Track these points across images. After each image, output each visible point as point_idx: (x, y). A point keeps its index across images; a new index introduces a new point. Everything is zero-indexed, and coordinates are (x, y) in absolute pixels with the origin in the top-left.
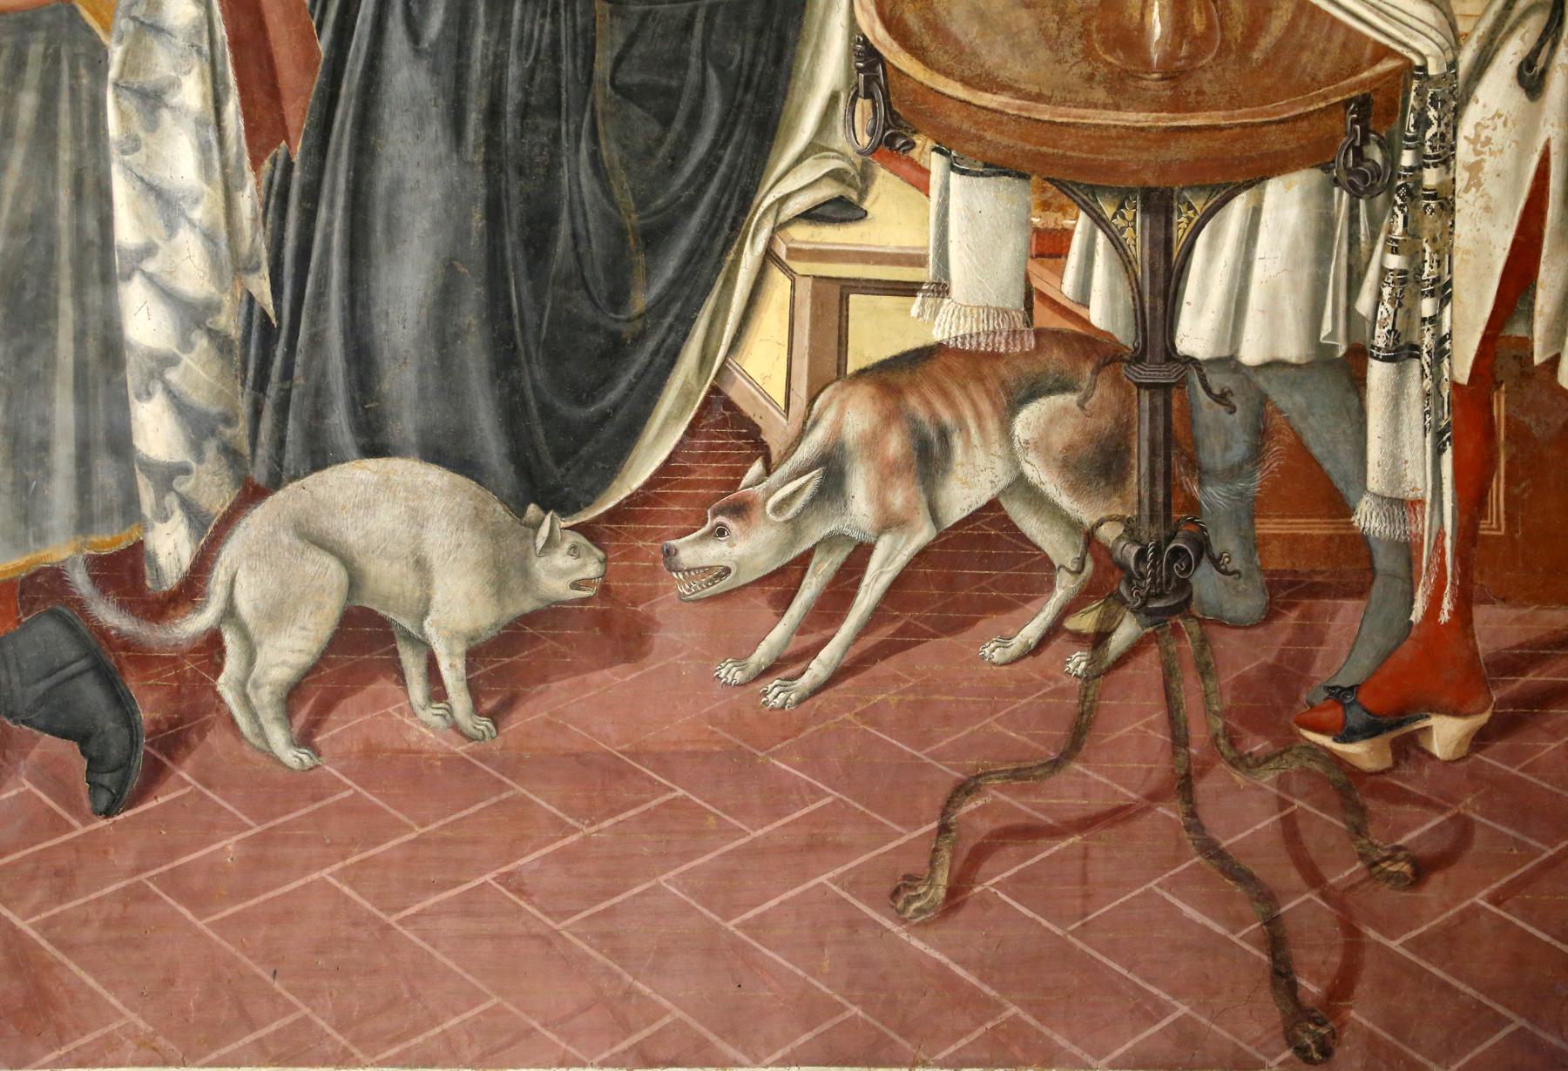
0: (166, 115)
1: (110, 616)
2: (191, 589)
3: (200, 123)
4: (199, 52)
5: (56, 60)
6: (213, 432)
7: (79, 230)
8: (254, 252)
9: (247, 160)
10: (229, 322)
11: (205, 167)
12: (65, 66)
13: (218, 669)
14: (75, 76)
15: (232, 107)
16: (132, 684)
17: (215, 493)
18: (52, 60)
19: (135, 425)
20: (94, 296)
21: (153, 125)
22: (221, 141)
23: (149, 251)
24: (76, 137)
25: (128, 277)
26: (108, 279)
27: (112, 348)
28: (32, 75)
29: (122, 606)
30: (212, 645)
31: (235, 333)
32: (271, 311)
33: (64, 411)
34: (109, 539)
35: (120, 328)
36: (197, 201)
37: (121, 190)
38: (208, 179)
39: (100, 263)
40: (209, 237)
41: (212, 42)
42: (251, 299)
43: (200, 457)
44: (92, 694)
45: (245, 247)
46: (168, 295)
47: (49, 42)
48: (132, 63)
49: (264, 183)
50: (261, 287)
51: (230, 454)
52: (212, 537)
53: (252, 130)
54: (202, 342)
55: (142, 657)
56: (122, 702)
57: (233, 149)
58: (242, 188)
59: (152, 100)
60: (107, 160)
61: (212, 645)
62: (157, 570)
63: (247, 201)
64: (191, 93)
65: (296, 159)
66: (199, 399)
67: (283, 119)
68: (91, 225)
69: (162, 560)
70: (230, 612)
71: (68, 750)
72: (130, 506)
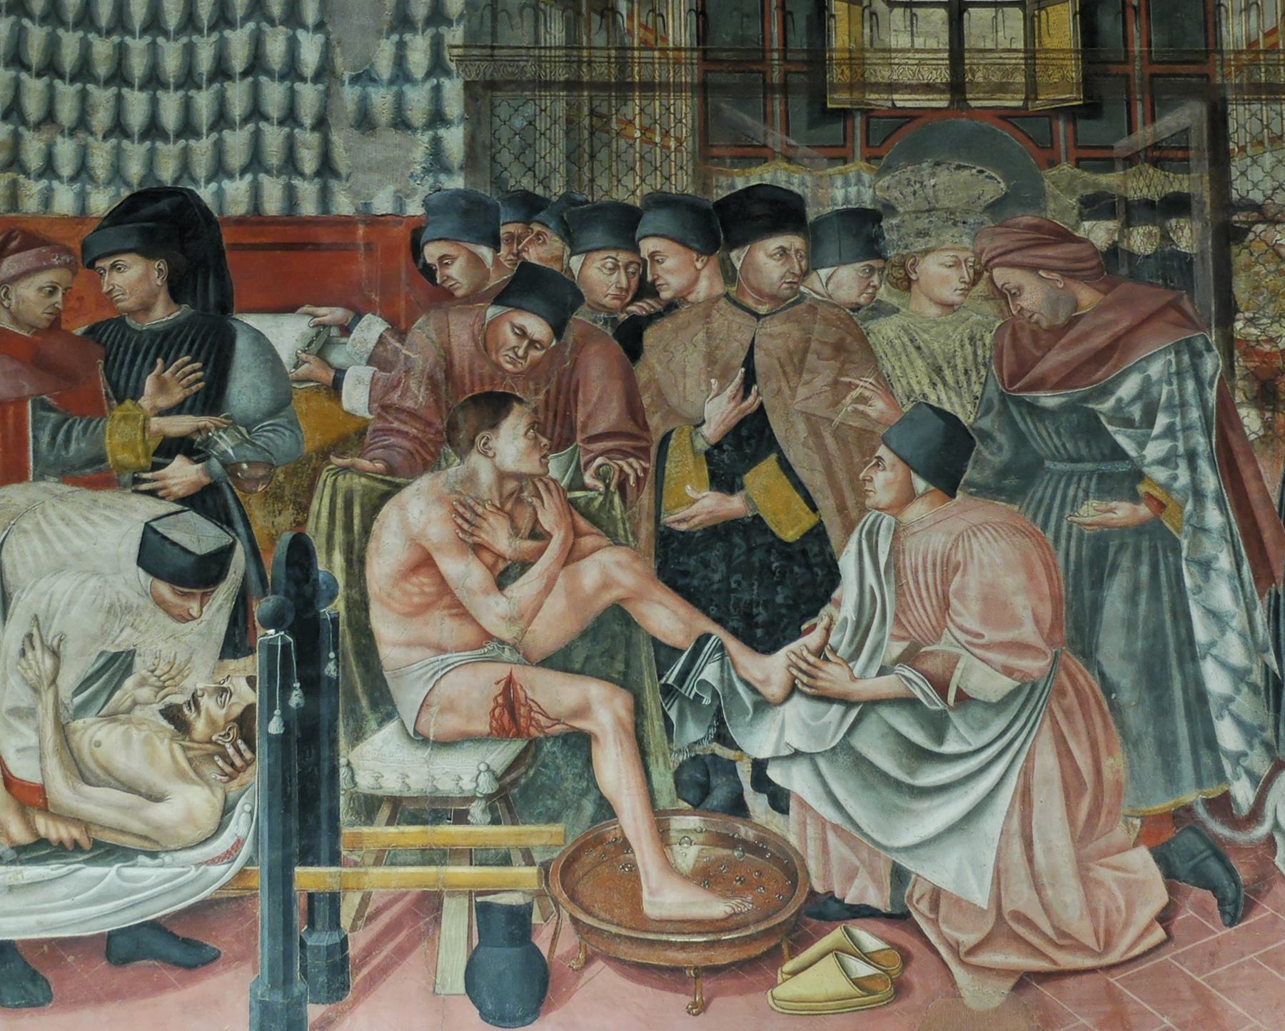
0: (1213, 574)
1: (1219, 829)
2: (1256, 814)
3: (1230, 577)
4: (1226, 541)
5: (1156, 549)
6: (1256, 735)
7: (1177, 634)
8: (1265, 643)
9: (1257, 598)
10: (1257, 677)
11: (1236, 599)
12: (1161, 553)
13: (1275, 853)
14: (1166, 557)
15: (1246, 568)
16: (1234, 862)
17: (1262, 765)
18: (1154, 550)
19: (1218, 733)
20: (1189, 667)
21: (1207, 577)
22: (1242, 586)
23: (1213, 644)
24: (1170, 588)
25: (1204, 658)
26: (1194, 659)
27: (1198, 695)
28: (1146, 558)
29: (1223, 823)
30: (1270, 842)
31: (1261, 684)
32: (1277, 672)
33: (1182, 729)
34: (1214, 791)
35: (1204, 684)
36: (1233, 617)
37: (1196, 613)
38: (1238, 605)
39: (1189, 651)
40: (1242, 635)
41: (1232, 535)
42: (1267, 666)
43: (1251, 747)
44: (1215, 868)
45: (1260, 639)
46: (1224, 665)
47: (1151, 540)
48: (1195, 546)
49: (1266, 603)
50: (1271, 658)
51: (1268, 747)
52: (1264, 787)
53: (1257, 580)
54: (1245, 689)
55: (1239, 849)
56: (1230, 871)
57: (1248, 589)
58: (1256, 608)
59: (1205, 566)
60: (1187, 600)
61: (1270, 842)
62: (1237, 804)
63: (1260, 616)
64: (1224, 561)
65: (1281, 592)
66: (1247, 718)
67: (1272, 572)
68: (1183, 632)
69: (1239, 800)
70: (1276, 825)
71: (1208, 894)
72: (1220, 775)
